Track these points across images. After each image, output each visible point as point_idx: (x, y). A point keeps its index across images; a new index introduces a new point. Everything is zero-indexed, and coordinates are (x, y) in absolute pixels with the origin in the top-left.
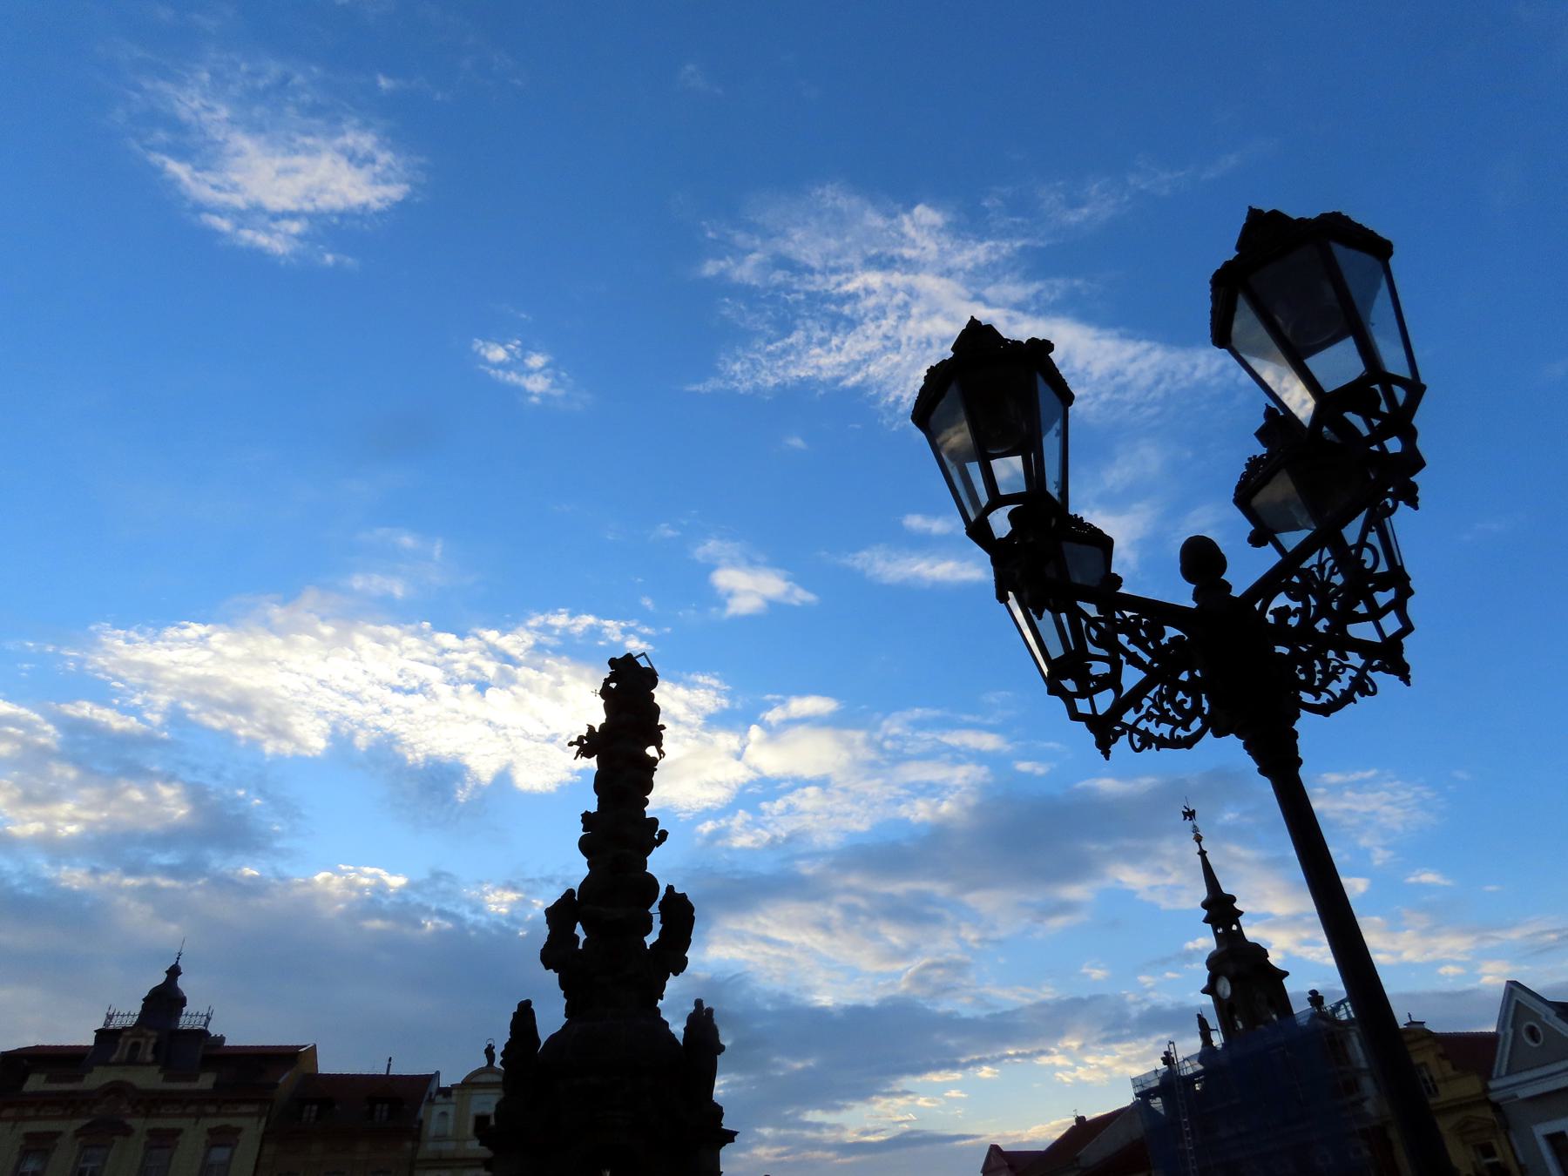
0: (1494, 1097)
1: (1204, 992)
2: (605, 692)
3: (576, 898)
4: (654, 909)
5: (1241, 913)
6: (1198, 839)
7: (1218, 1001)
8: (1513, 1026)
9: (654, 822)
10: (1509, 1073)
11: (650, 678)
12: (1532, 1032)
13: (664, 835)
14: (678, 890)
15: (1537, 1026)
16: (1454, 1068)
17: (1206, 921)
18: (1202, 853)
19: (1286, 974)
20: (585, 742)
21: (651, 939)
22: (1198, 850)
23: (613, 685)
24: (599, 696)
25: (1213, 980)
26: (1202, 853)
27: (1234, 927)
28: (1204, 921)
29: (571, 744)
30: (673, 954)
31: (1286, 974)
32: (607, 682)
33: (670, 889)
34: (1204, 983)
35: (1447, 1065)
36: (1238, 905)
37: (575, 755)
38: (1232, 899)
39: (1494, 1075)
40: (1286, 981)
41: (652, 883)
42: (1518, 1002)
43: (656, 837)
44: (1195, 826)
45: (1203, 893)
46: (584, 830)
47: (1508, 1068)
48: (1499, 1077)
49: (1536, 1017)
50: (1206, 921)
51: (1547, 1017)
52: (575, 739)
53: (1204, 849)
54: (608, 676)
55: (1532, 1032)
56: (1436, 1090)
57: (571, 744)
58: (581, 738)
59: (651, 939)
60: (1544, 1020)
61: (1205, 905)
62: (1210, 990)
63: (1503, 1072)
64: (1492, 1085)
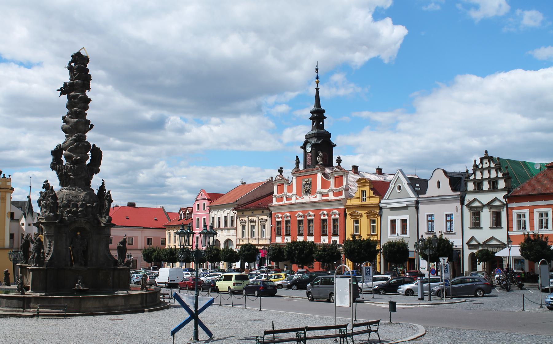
0: (381, 205)
1: (301, 147)
2: (70, 68)
3: (61, 147)
4: (89, 154)
5: (325, 118)
6: (317, 83)
7: (305, 153)
8: (394, 184)
9: (89, 122)
10: (388, 199)
11: (86, 60)
12: (399, 188)
13: (92, 126)
14: (97, 146)
15: (401, 186)
16: (374, 194)
17: (310, 119)
18: (317, 89)
19: (336, 145)
20: (63, 89)
21: (88, 162)
22: (316, 87)
23: (73, 64)
24: (67, 68)
25: (306, 143)
26: (317, 89)
27: (321, 123)
28: (309, 119)
29: (58, 90)
30: (95, 167)
31: (336, 145)
32: (70, 63)
33: (94, 145)
34: (302, 145)
35: (372, 192)
36: (325, 114)
37: (60, 95)
38: (324, 111)
39: (384, 199)
40: (334, 148)
41: (89, 144)
42: (399, 177)
43: (89, 127)
44: (318, 76)
45: (313, 107)
46: (63, 123)
47: (388, 198)
48: (385, 199)
49: (402, 183)
50: (310, 119)
51: (405, 184)
52: (59, 89)
53: (319, 88)
54: (70, 60)
55: (399, 188)
57: (58, 90)
58: (61, 88)
59: (88, 162)
60: (403, 184)
61: (312, 112)
62: (304, 147)
63: (386, 199)
64: (382, 202)
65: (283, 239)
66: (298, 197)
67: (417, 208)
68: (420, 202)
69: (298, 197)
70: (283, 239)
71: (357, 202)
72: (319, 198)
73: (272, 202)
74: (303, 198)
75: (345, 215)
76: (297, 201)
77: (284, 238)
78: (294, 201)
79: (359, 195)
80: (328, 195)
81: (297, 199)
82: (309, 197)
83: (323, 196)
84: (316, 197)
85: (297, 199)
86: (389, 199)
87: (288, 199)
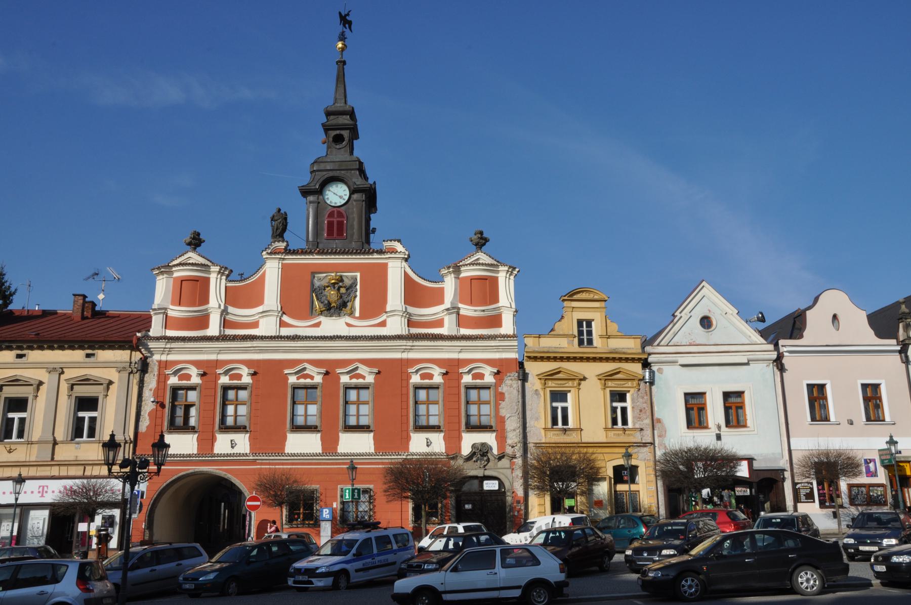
48: (658, 345)
56: (590, 342)
65: (207, 442)
66: (285, 318)
67: (781, 369)
68: (785, 354)
69: (285, 318)
70: (207, 442)
71: (568, 345)
72: (396, 325)
73: (148, 327)
74: (318, 325)
75: (524, 378)
76: (285, 332)
77: (213, 440)
78: (268, 327)
79: (569, 325)
80: (439, 323)
81: (282, 324)
82: (348, 325)
83: (410, 324)
84: (383, 324)
85: (282, 324)
86: (669, 344)
87: (225, 323)
